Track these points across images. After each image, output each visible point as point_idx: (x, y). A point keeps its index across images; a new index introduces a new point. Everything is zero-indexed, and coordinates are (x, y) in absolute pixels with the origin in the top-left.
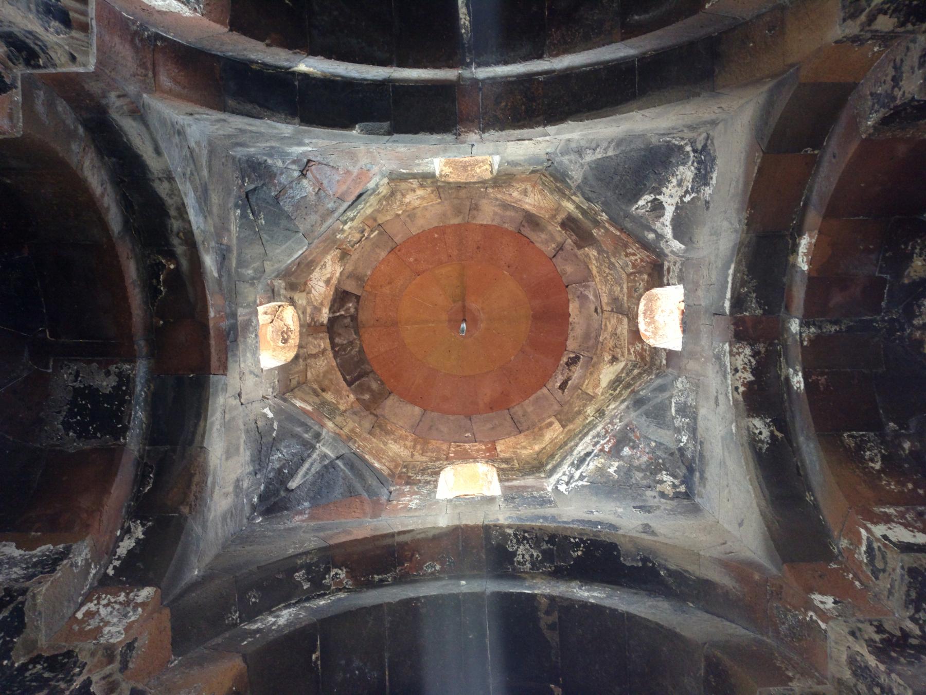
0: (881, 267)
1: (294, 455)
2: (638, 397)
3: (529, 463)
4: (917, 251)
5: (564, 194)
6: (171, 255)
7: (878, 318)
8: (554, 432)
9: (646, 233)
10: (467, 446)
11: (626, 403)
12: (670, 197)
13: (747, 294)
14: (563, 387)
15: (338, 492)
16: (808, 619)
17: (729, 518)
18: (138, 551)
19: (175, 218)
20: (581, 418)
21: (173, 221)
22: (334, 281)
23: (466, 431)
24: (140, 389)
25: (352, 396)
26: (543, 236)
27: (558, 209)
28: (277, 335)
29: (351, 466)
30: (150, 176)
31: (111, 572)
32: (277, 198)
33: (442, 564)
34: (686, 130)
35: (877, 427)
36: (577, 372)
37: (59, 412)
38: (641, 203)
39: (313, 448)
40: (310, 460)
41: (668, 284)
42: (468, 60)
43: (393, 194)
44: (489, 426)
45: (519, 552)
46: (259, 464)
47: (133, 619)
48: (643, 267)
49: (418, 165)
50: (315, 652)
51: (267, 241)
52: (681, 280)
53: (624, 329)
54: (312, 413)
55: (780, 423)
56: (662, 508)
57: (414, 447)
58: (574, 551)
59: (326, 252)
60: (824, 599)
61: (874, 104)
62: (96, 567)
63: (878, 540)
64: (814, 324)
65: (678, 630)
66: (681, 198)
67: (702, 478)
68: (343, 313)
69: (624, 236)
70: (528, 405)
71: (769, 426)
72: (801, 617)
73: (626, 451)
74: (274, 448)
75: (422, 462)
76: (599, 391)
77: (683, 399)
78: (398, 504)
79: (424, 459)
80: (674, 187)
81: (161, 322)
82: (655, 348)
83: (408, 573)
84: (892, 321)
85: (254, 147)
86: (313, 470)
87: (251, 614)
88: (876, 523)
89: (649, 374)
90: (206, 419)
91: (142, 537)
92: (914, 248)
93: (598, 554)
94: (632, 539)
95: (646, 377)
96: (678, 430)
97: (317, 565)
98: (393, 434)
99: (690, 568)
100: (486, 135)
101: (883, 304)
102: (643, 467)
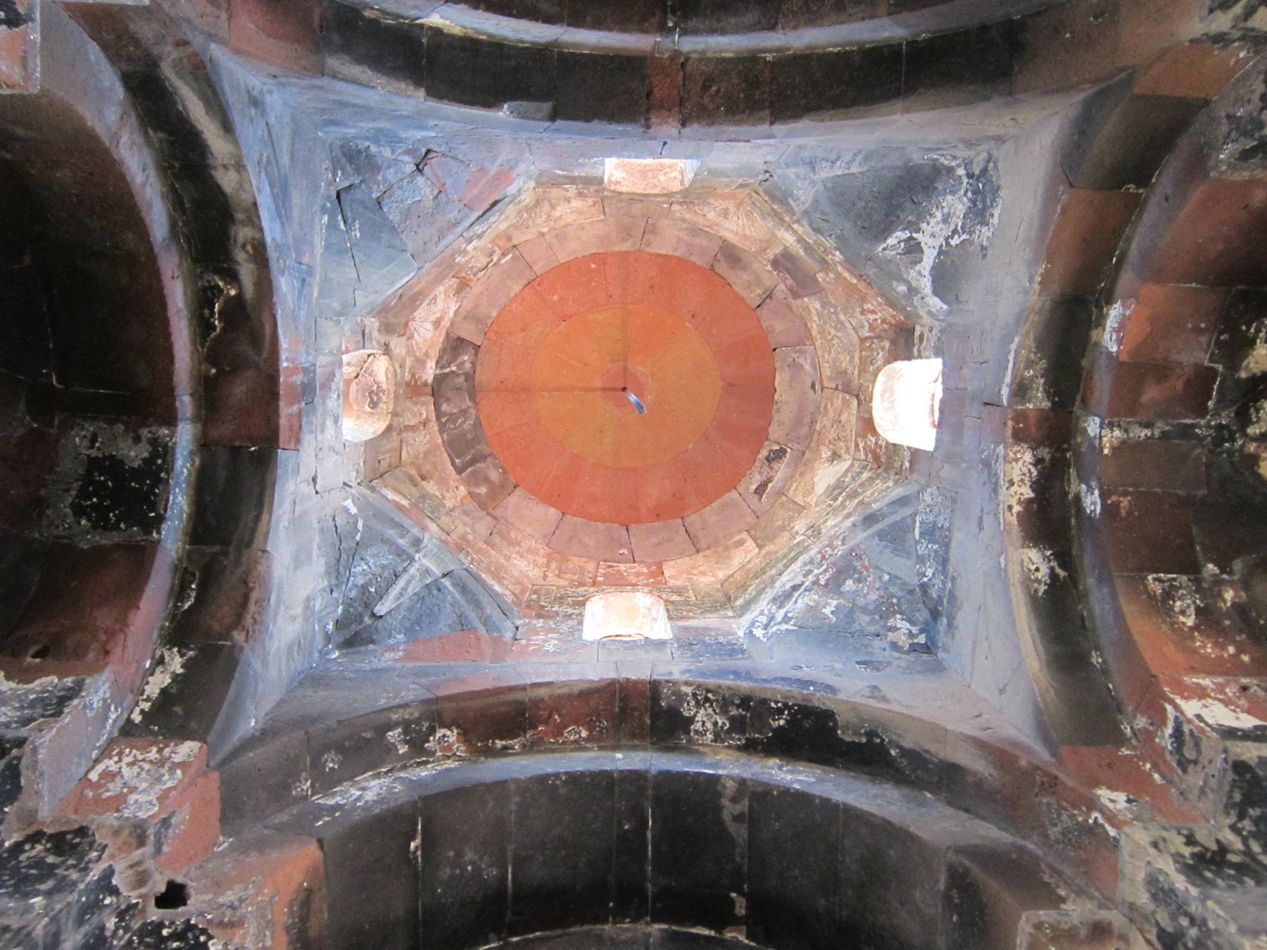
0: (1212, 354)
1: (383, 567)
2: (869, 511)
3: (710, 596)
4: (1262, 335)
5: (782, 220)
6: (232, 276)
7: (1203, 422)
8: (746, 554)
9: (895, 284)
10: (622, 567)
11: (852, 519)
12: (931, 236)
13: (1032, 379)
14: (760, 491)
15: (444, 624)
16: (1091, 821)
17: (984, 684)
18: (174, 691)
20: (786, 535)
22: (446, 323)
23: (621, 546)
24: (183, 465)
25: (462, 488)
26: (745, 276)
27: (772, 239)
28: (363, 395)
29: (464, 589)
30: (210, 161)
31: (137, 717)
32: (379, 202)
33: (591, 729)
34: (961, 146)
35: (1193, 569)
36: (781, 470)
37: (67, 490)
38: (891, 241)
39: (412, 559)
41: (920, 357)
42: (670, 24)
43: (538, 203)
44: (654, 540)
45: (699, 718)
47: (169, 784)
48: (885, 330)
49: (583, 165)
50: (413, 838)
51: (362, 262)
52: (938, 352)
53: (851, 416)
54: (408, 510)
55: (1064, 557)
56: (895, 663)
57: (548, 565)
58: (774, 720)
59: (438, 280)
60: (1114, 795)
61: (1231, 131)
63: (1189, 721)
64: (1119, 426)
65: (912, 829)
66: (947, 240)
67: (950, 625)
68: (454, 368)
69: (862, 286)
70: (710, 513)
71: (1050, 561)
72: (1080, 819)
73: (849, 585)
74: (357, 557)
75: (558, 588)
76: (812, 500)
77: (931, 518)
78: (527, 645)
79: (562, 582)
80: (938, 223)
81: (214, 371)
82: (894, 445)
83: (541, 739)
84: (1220, 427)
85: (355, 127)
86: (410, 591)
87: (327, 783)
88: (1186, 698)
89: (885, 480)
90: (271, 513)
91: (180, 671)
92: (1258, 331)
93: (807, 724)
94: (854, 708)
95: (879, 484)
96: (921, 560)
97: (418, 722)
98: (519, 544)
99: (933, 748)
100: (686, 131)
101: (1211, 404)
102: (871, 607)
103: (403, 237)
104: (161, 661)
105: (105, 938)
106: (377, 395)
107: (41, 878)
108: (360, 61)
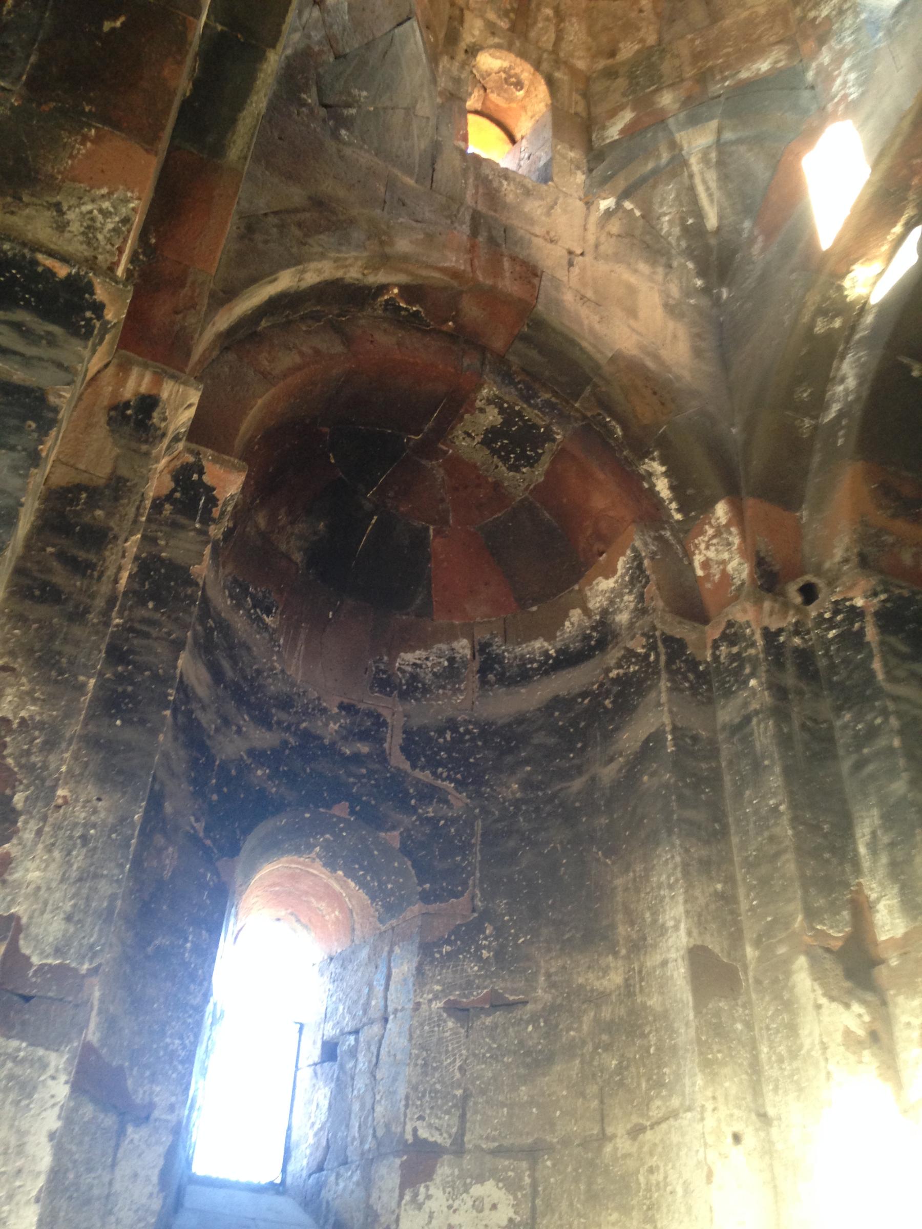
6: (383, 288)
19: (345, 273)
21: (348, 276)
28: (506, 91)
37: (497, 467)
40: (698, 180)
46: (663, 255)
62: (664, 529)
74: (654, 222)
86: (713, 185)
91: (663, 469)
103: (378, 34)
104: (650, 474)
105: (804, 650)
106: (510, 76)
107: (741, 667)
108: (233, 121)
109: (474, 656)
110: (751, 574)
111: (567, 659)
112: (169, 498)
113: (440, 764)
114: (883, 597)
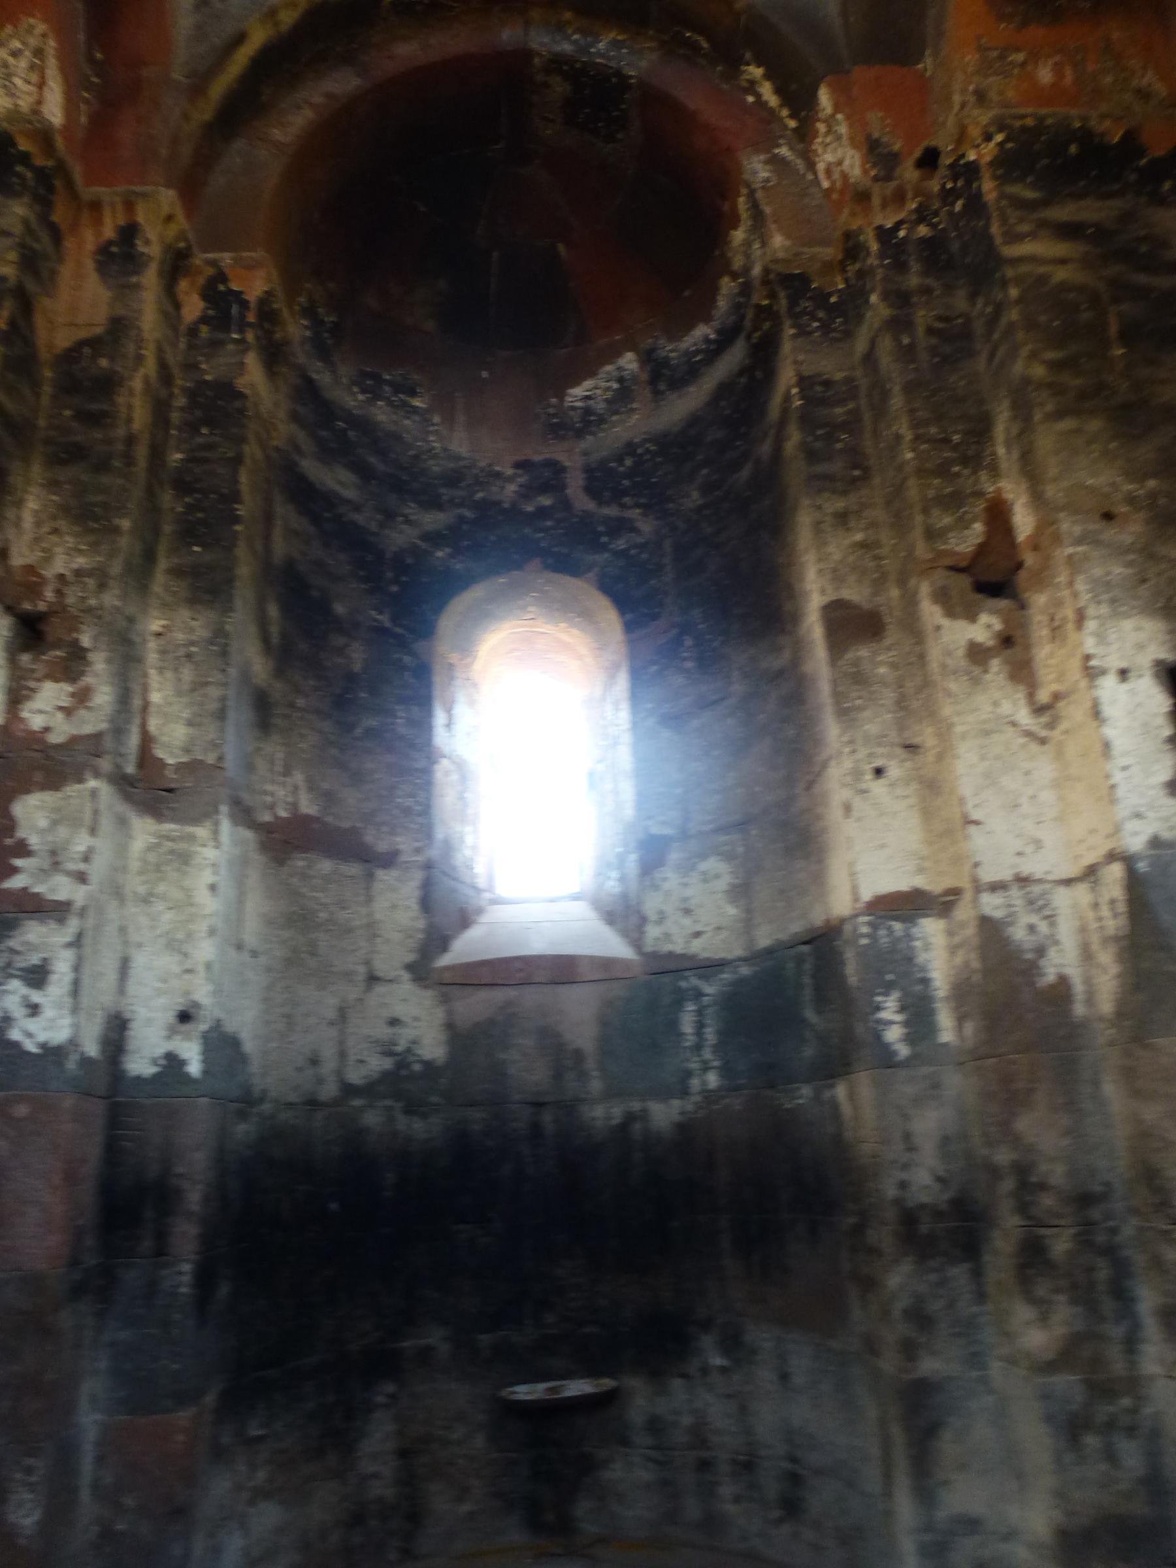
62: (779, 146)
104: (752, 83)
109: (642, 368)
110: (863, 165)
111: (726, 338)
112: (204, 320)
113: (625, 493)
114: (999, 138)
